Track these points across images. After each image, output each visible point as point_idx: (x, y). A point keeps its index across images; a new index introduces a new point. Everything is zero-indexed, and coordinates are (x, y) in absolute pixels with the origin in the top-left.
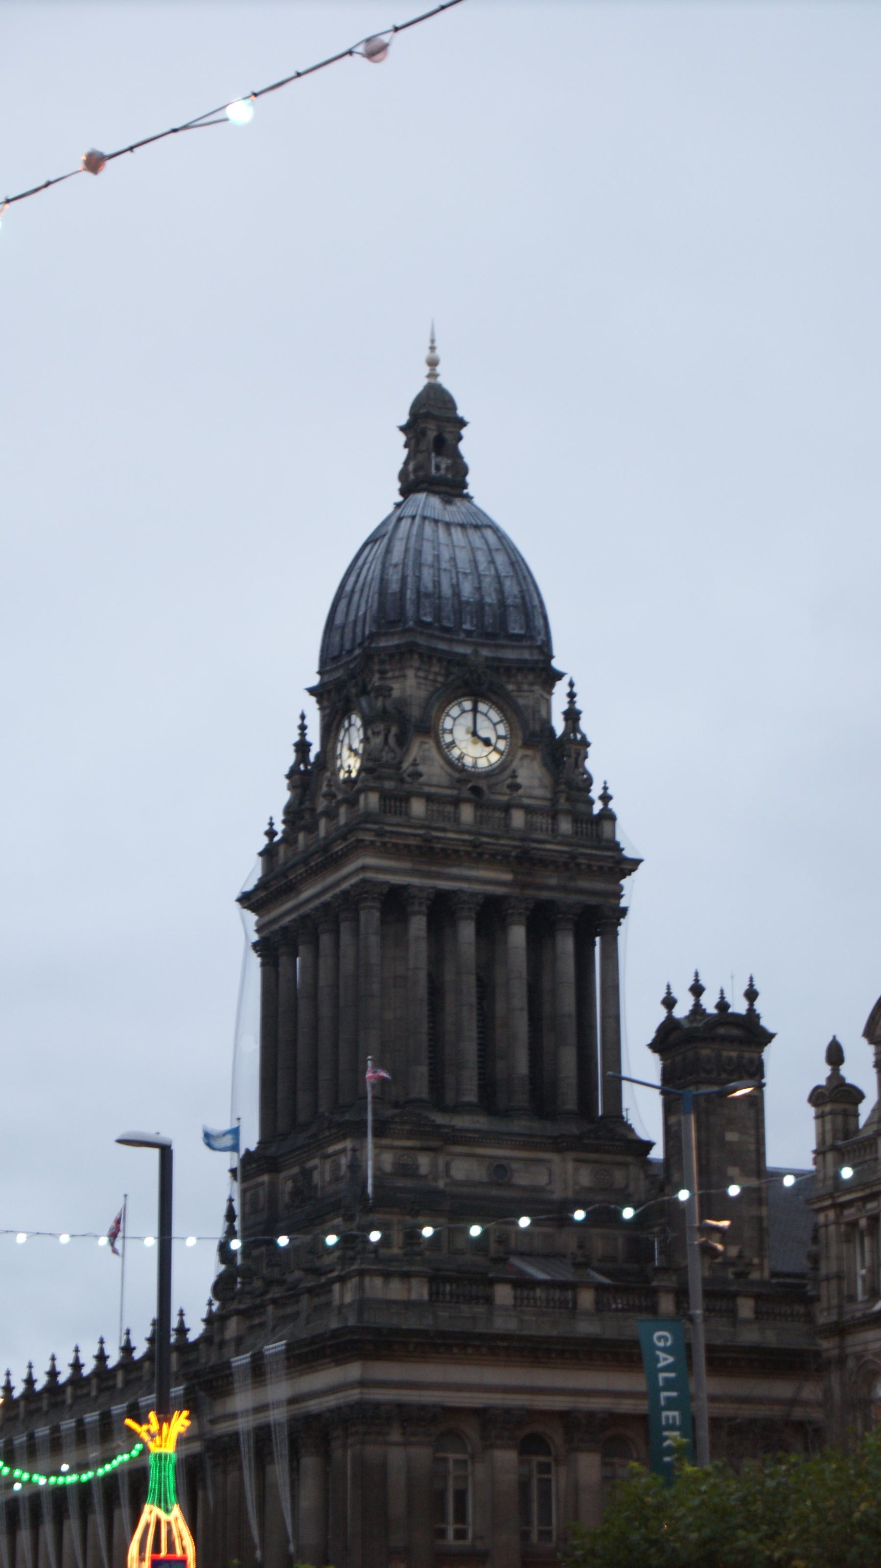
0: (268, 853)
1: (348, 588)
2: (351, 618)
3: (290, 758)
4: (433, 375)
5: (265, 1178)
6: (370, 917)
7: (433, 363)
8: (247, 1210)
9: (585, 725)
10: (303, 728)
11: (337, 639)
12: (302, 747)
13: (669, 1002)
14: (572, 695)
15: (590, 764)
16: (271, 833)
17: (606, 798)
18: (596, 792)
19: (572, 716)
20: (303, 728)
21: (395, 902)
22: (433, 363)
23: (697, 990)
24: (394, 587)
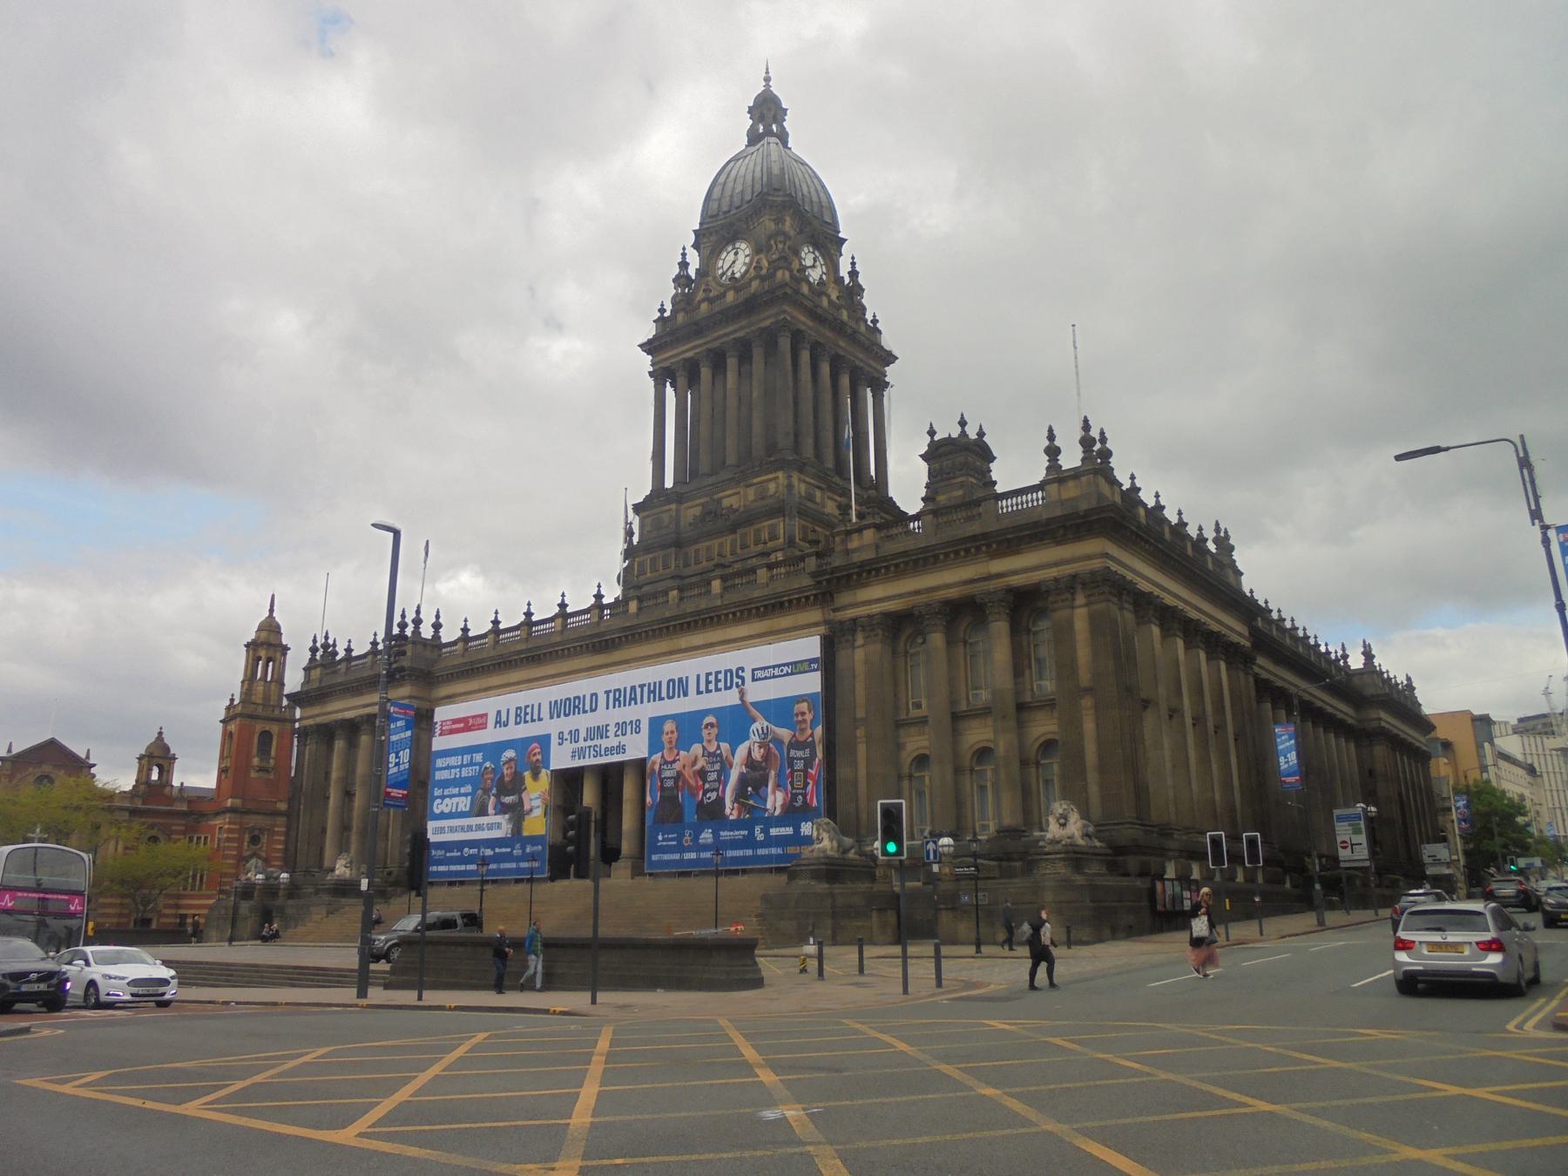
0: (661, 321)
1: (722, 179)
2: (728, 193)
3: (676, 270)
4: (767, 86)
5: (673, 506)
6: (785, 343)
7: (767, 79)
8: (648, 528)
9: (861, 280)
10: (684, 255)
11: (715, 205)
12: (684, 265)
13: (932, 433)
14: (853, 264)
15: (866, 301)
16: (662, 310)
17: (875, 321)
18: (869, 317)
19: (854, 274)
20: (684, 255)
21: (797, 337)
22: (767, 79)
23: (963, 423)
24: (776, 171)
